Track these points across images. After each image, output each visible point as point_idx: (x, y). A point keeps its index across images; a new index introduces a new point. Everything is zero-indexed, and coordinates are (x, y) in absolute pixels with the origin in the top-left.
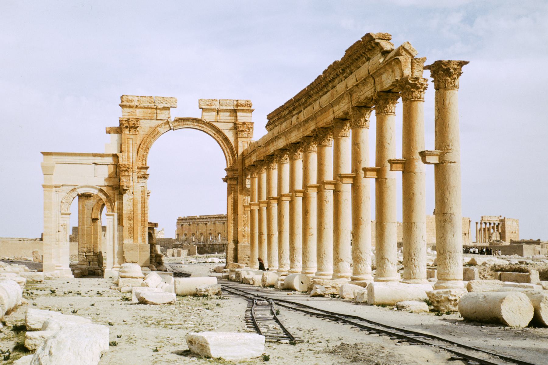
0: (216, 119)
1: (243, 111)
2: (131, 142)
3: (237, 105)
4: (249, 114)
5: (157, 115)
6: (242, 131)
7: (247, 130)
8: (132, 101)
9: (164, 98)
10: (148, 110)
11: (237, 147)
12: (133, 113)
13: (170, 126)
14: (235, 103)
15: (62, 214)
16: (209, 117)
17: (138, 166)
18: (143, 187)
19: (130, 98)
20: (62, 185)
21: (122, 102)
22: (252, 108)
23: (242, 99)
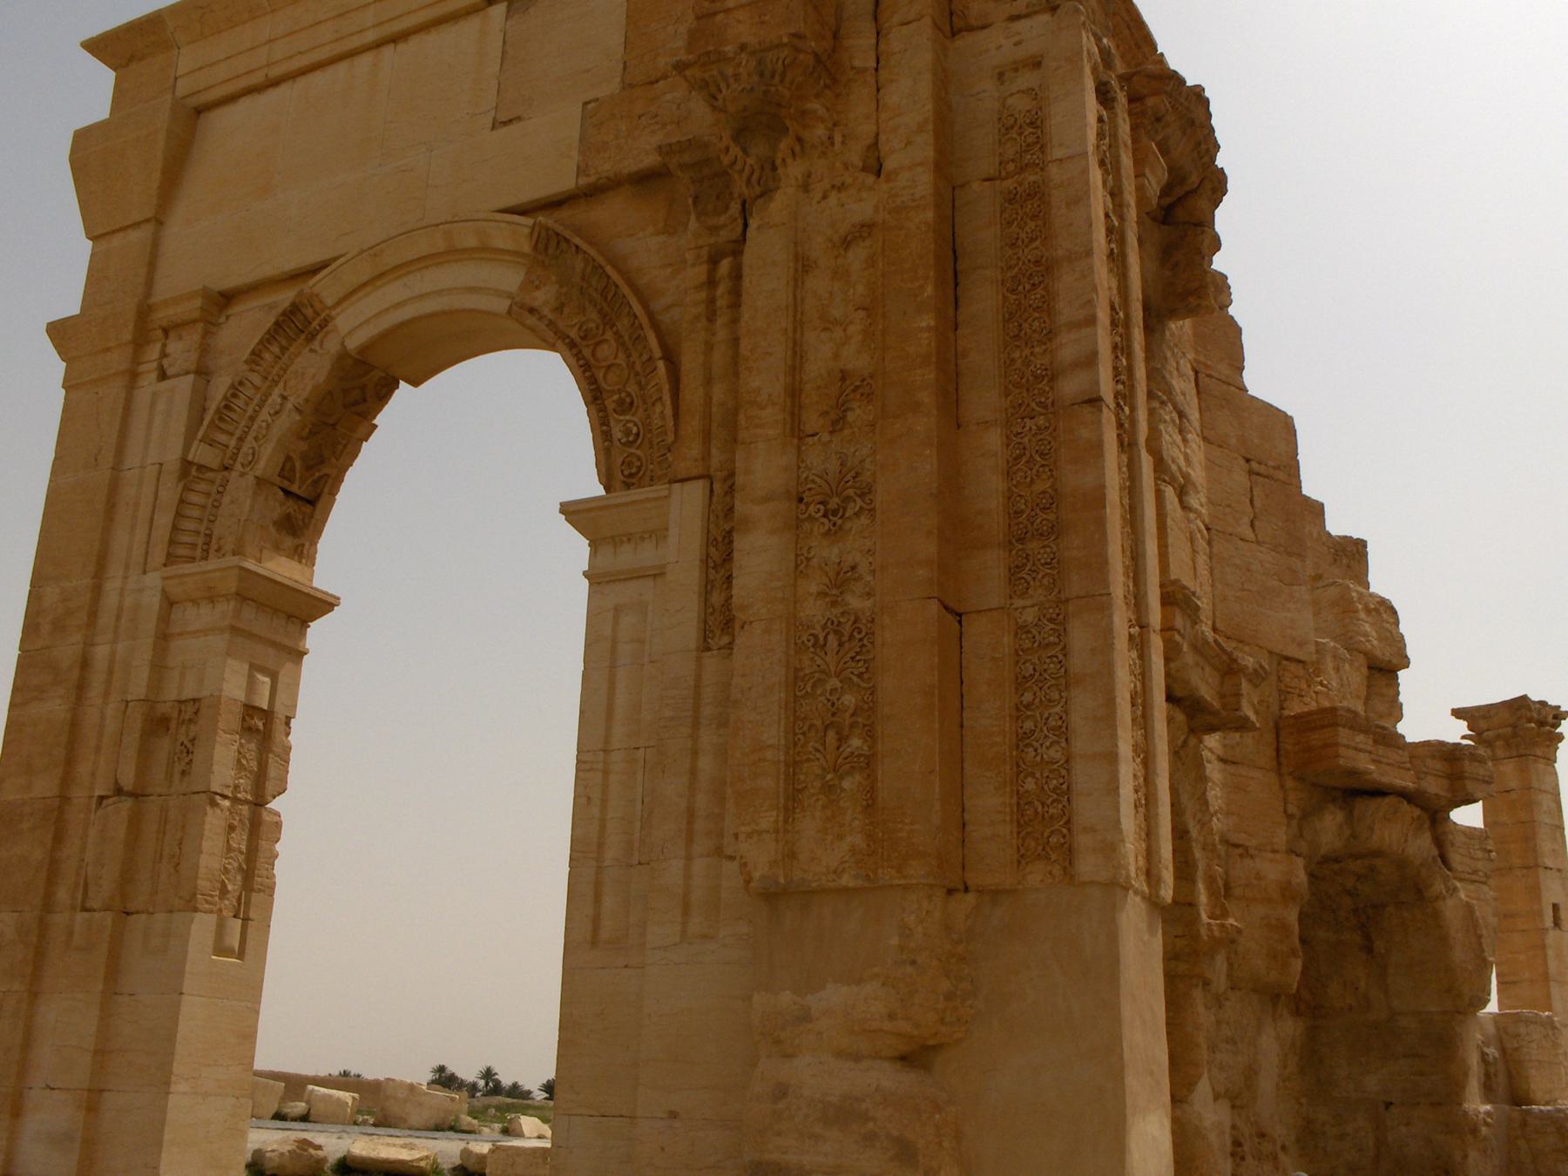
18: (1036, 63)
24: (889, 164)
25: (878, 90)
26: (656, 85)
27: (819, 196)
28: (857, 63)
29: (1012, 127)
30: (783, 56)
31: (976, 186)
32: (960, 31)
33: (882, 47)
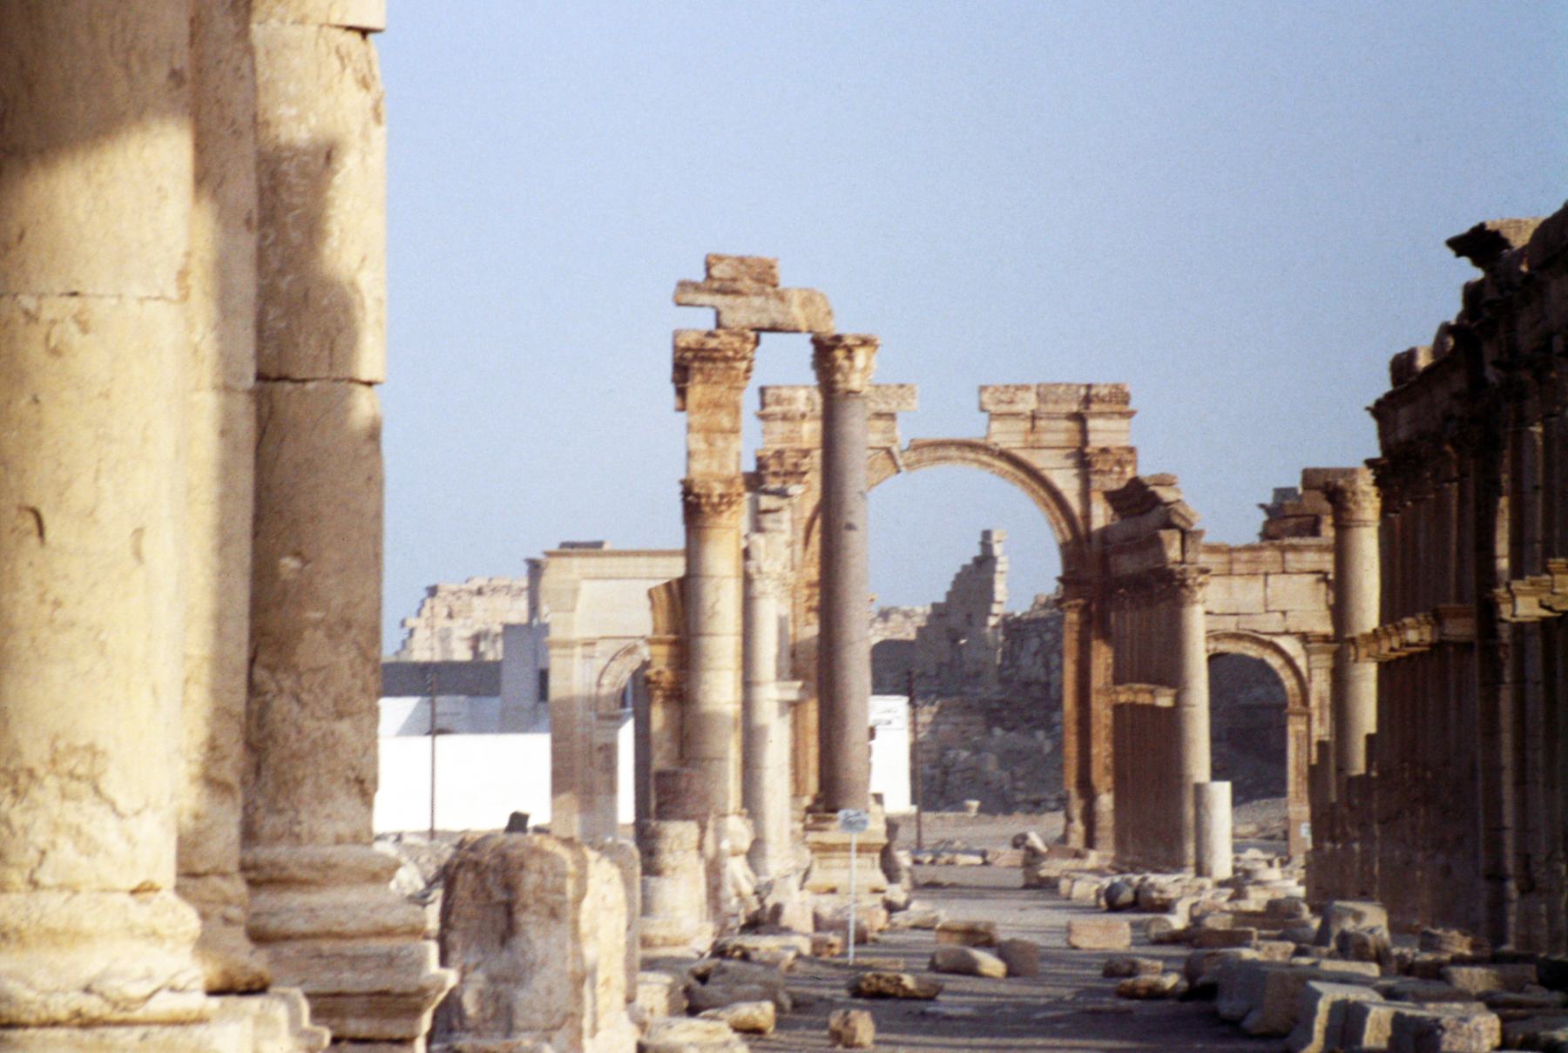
0: (1026, 441)
1: (1101, 414)
3: (1087, 400)
4: (1122, 424)
8: (791, 401)
9: (883, 389)
11: (1087, 516)
14: (1083, 392)
15: (601, 717)
16: (1008, 436)
19: (785, 393)
20: (603, 638)
21: (763, 405)
22: (1131, 407)
23: (1102, 382)
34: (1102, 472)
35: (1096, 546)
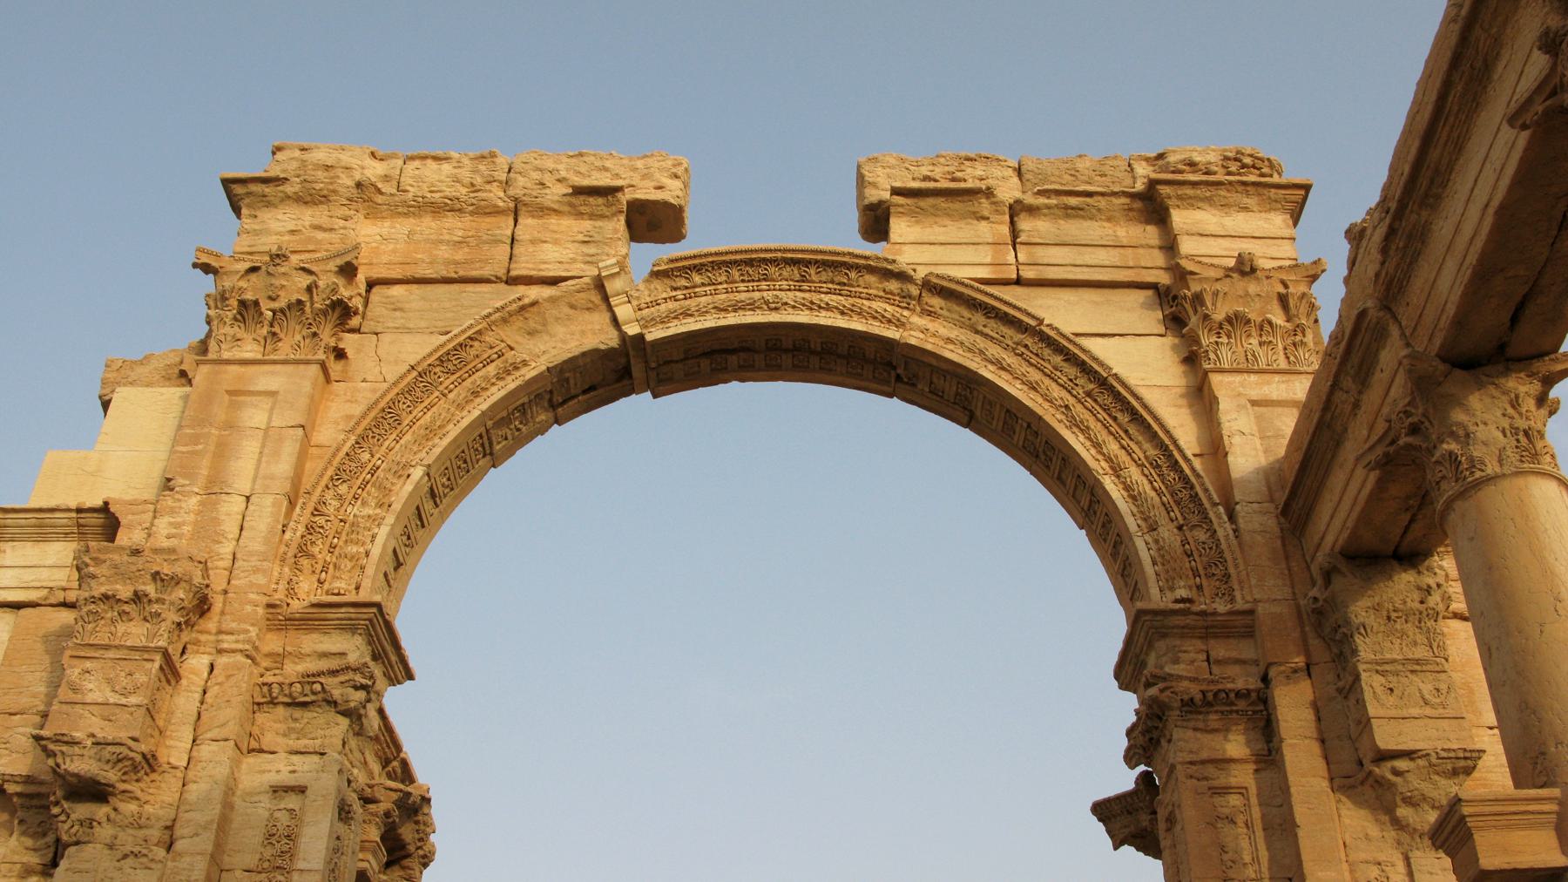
2: (255, 416)
5: (516, 251)
6: (1236, 321)
7: (1278, 319)
10: (450, 221)
11: (1216, 449)
12: (320, 235)
13: (615, 322)
17: (279, 596)
18: (301, 790)
24: (178, 846)
25: (184, 785)
26: (13, 717)
27: (119, 855)
28: (173, 761)
29: (274, 835)
30: (118, 752)
31: (238, 873)
32: (253, 750)
33: (194, 754)
34: (1236, 321)
35: (1257, 520)
